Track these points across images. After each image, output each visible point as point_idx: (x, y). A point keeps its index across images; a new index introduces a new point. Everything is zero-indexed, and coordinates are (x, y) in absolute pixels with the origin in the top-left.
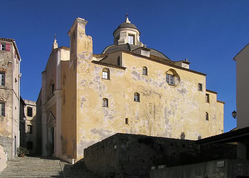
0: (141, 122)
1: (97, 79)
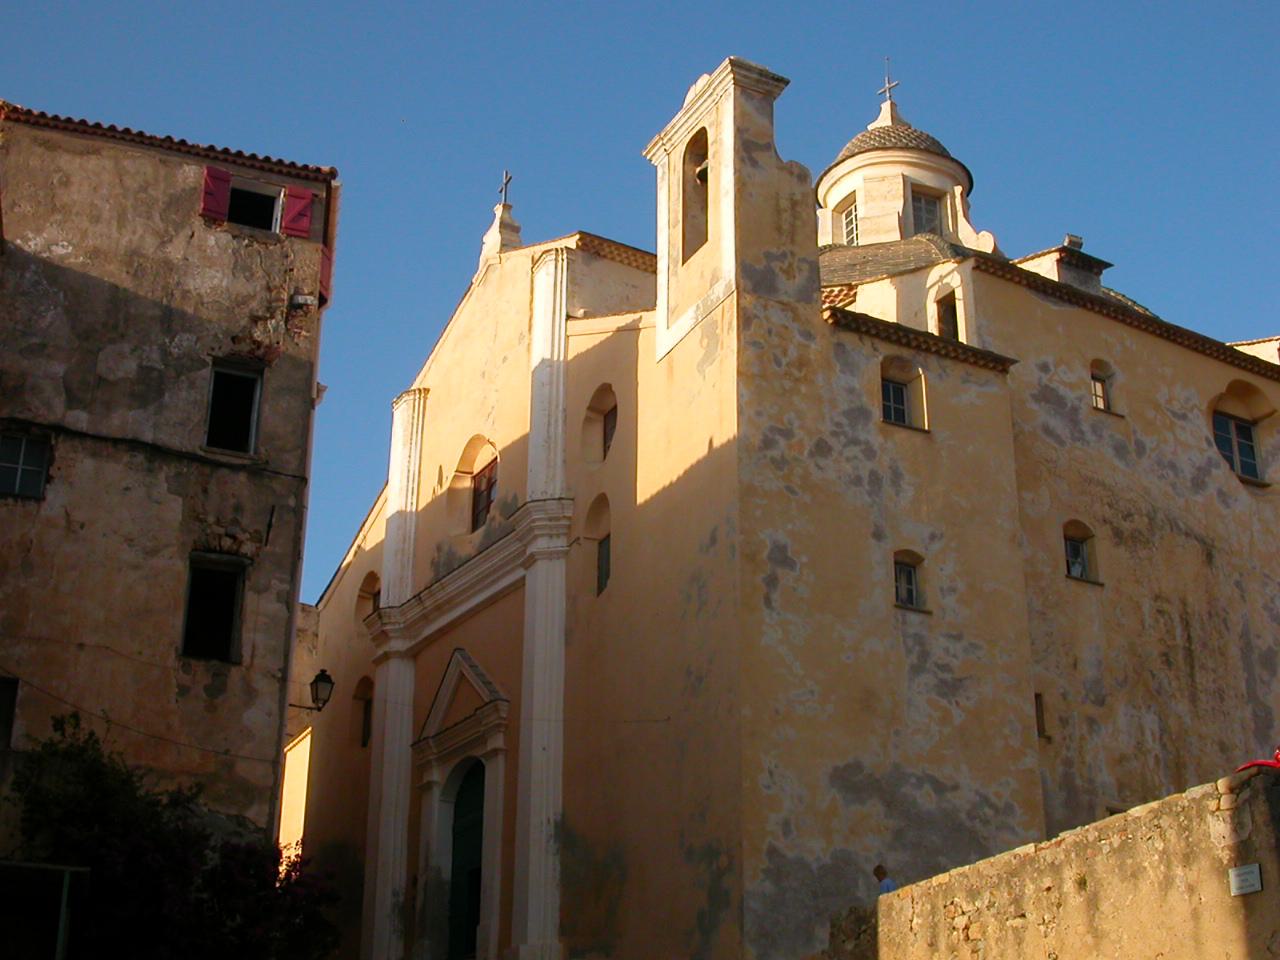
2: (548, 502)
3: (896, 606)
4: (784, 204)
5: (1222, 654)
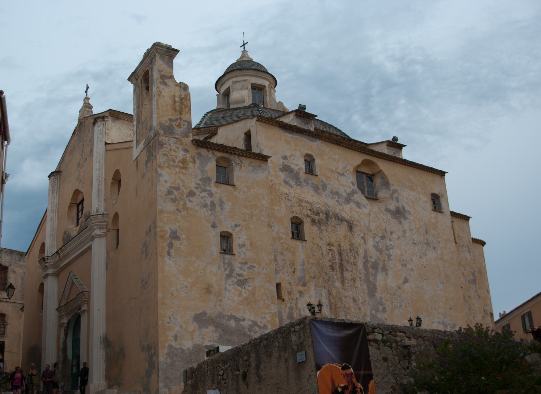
0: (313, 292)
1: (205, 186)
2: (98, 216)
3: (220, 253)
4: (177, 99)
5: (355, 265)
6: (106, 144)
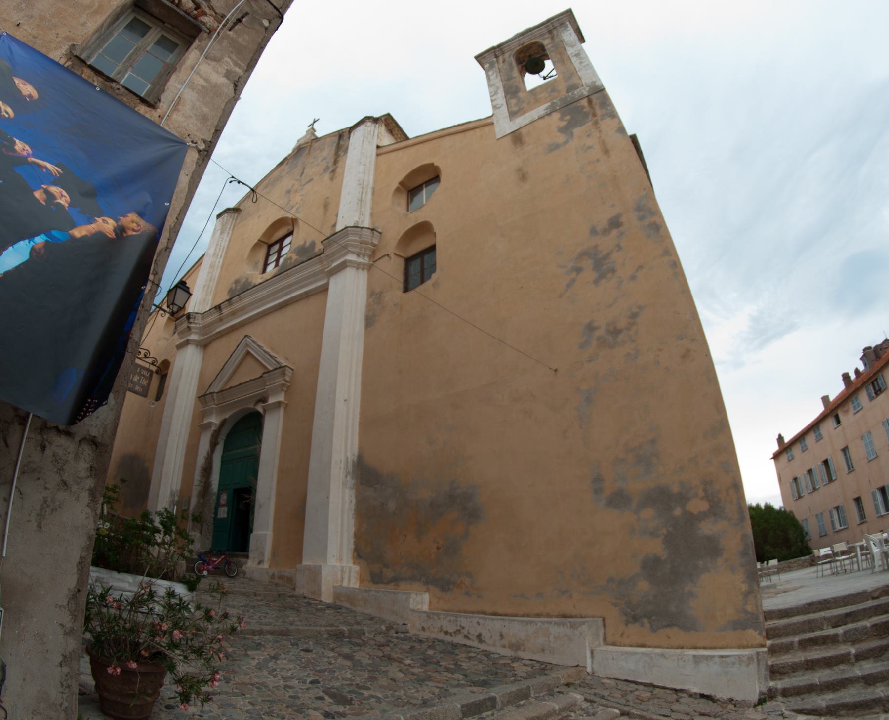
6: (378, 147)
